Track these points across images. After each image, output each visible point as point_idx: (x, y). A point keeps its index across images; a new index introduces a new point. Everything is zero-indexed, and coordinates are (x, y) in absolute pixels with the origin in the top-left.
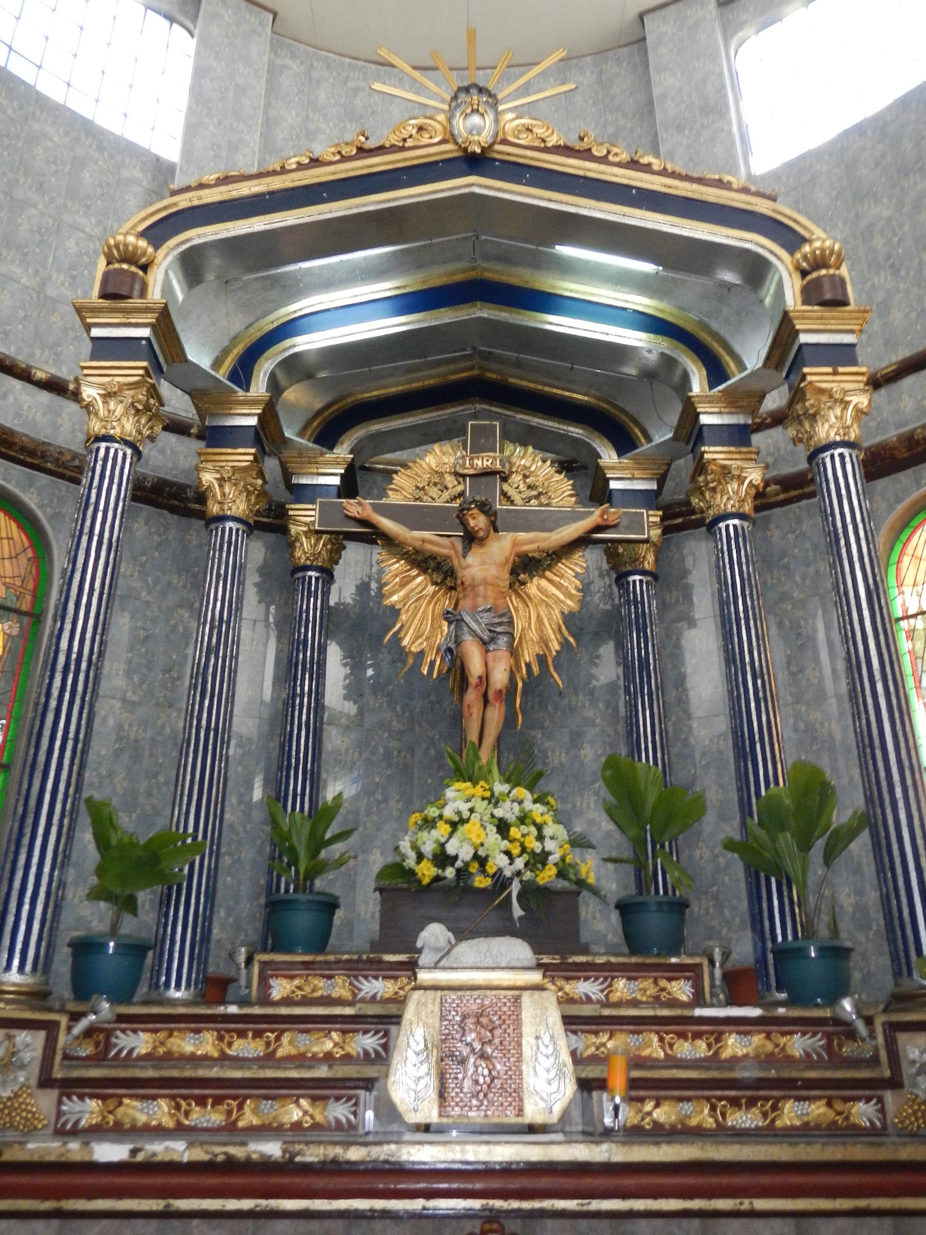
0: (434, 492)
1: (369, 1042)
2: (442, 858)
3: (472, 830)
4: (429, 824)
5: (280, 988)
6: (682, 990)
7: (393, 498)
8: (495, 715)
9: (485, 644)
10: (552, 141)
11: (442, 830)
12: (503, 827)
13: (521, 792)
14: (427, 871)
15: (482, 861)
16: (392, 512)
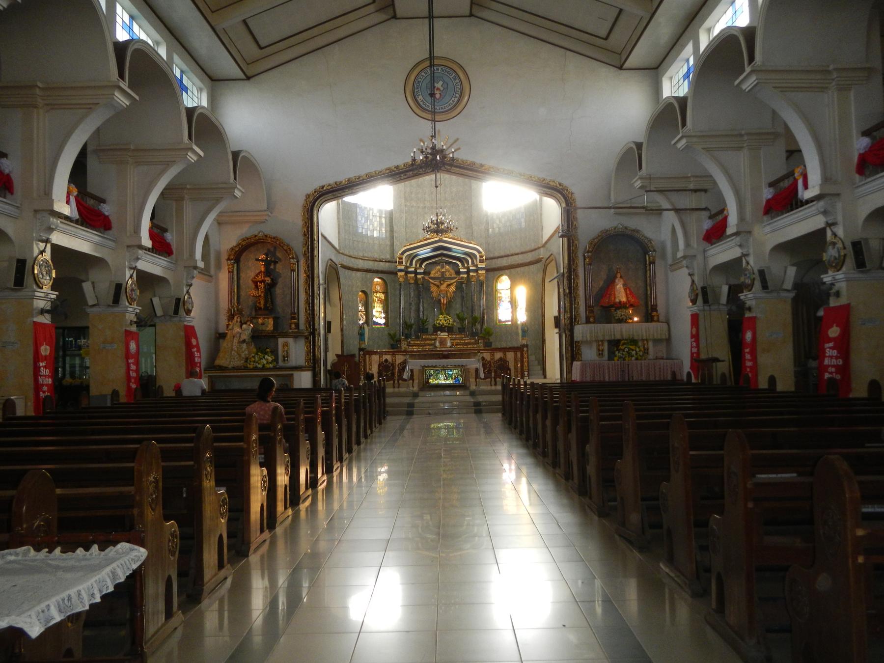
0: (436, 274)
1: (433, 342)
2: (439, 324)
3: (442, 321)
4: (437, 320)
5: (424, 337)
6: (463, 336)
7: (432, 275)
8: (445, 307)
9: (443, 298)
10: (451, 236)
11: (439, 321)
12: (445, 321)
13: (448, 316)
14: (438, 325)
15: (443, 324)
16: (431, 278)
